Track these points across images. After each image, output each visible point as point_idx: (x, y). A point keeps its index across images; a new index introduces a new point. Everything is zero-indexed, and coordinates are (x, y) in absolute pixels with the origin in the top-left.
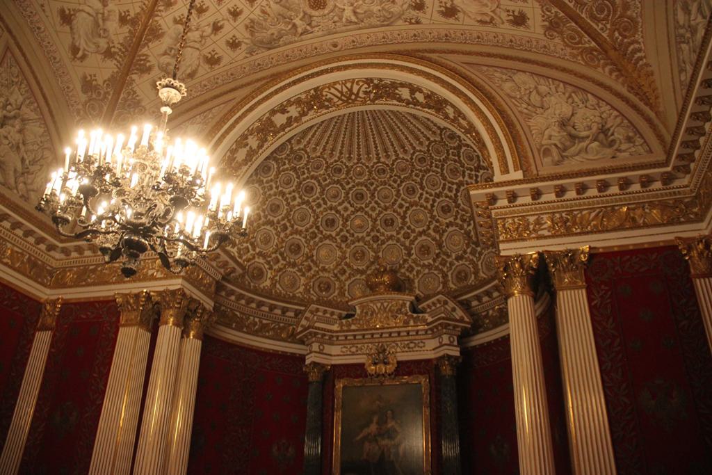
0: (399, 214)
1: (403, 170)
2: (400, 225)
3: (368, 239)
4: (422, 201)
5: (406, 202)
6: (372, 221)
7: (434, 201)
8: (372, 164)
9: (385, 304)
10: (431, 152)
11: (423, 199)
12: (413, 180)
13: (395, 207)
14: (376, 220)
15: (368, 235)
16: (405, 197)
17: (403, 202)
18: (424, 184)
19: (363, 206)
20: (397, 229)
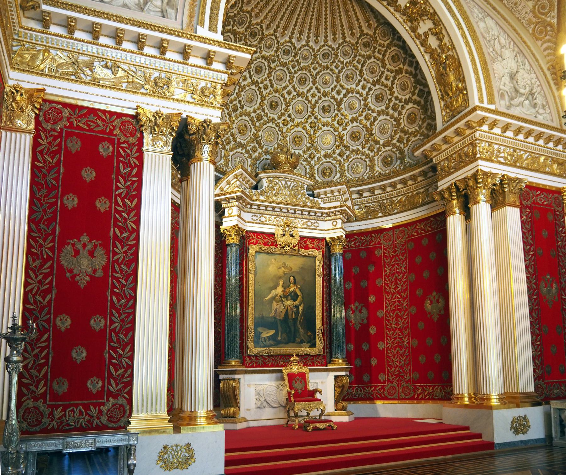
0: (285, 100)
1: (305, 58)
2: (283, 111)
3: (253, 115)
4: (309, 95)
5: (295, 91)
6: (261, 98)
7: (320, 98)
8: (282, 41)
9: (289, 183)
10: (339, 51)
11: (311, 93)
12: (310, 71)
13: (285, 92)
14: (265, 99)
15: (255, 111)
16: (296, 86)
17: (292, 90)
18: (317, 80)
19: (259, 80)
20: (279, 114)
